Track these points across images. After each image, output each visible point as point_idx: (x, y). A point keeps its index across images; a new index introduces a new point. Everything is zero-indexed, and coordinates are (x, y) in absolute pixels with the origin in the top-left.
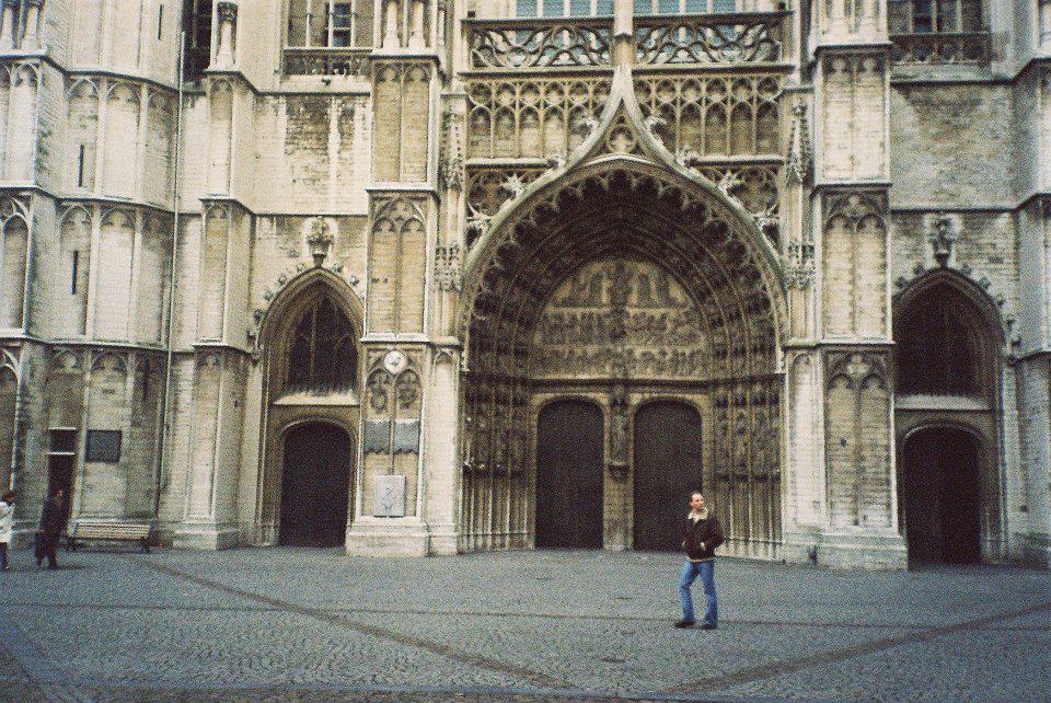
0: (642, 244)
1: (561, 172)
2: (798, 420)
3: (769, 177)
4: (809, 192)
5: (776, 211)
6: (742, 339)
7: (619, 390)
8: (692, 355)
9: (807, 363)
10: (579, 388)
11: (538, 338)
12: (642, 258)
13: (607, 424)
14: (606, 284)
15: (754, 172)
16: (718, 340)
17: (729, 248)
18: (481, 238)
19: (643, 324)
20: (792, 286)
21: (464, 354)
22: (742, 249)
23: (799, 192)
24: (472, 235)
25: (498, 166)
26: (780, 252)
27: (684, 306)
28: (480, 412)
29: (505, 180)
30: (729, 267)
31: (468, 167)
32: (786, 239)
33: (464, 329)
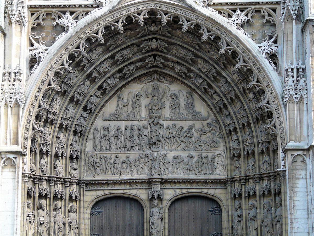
0: (173, 69)
1: (105, 9)
2: (296, 208)
3: (269, 15)
4: (301, 26)
5: (275, 42)
6: (252, 144)
7: (156, 188)
8: (213, 158)
9: (303, 161)
10: (123, 187)
11: (89, 147)
12: (173, 79)
13: (146, 215)
14: (144, 102)
15: (258, 11)
16: (234, 145)
17: (240, 71)
18: (41, 64)
19: (174, 133)
20: (291, 100)
21: (27, 159)
22: (250, 71)
23: (295, 27)
24: (33, 62)
25: (54, 7)
26: (280, 74)
27: (207, 118)
28: (40, 208)
29: (60, 18)
30: (241, 87)
31: (30, 7)
32: (284, 63)
33: (26, 138)
